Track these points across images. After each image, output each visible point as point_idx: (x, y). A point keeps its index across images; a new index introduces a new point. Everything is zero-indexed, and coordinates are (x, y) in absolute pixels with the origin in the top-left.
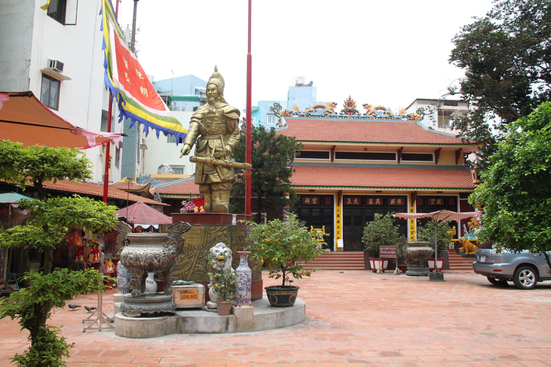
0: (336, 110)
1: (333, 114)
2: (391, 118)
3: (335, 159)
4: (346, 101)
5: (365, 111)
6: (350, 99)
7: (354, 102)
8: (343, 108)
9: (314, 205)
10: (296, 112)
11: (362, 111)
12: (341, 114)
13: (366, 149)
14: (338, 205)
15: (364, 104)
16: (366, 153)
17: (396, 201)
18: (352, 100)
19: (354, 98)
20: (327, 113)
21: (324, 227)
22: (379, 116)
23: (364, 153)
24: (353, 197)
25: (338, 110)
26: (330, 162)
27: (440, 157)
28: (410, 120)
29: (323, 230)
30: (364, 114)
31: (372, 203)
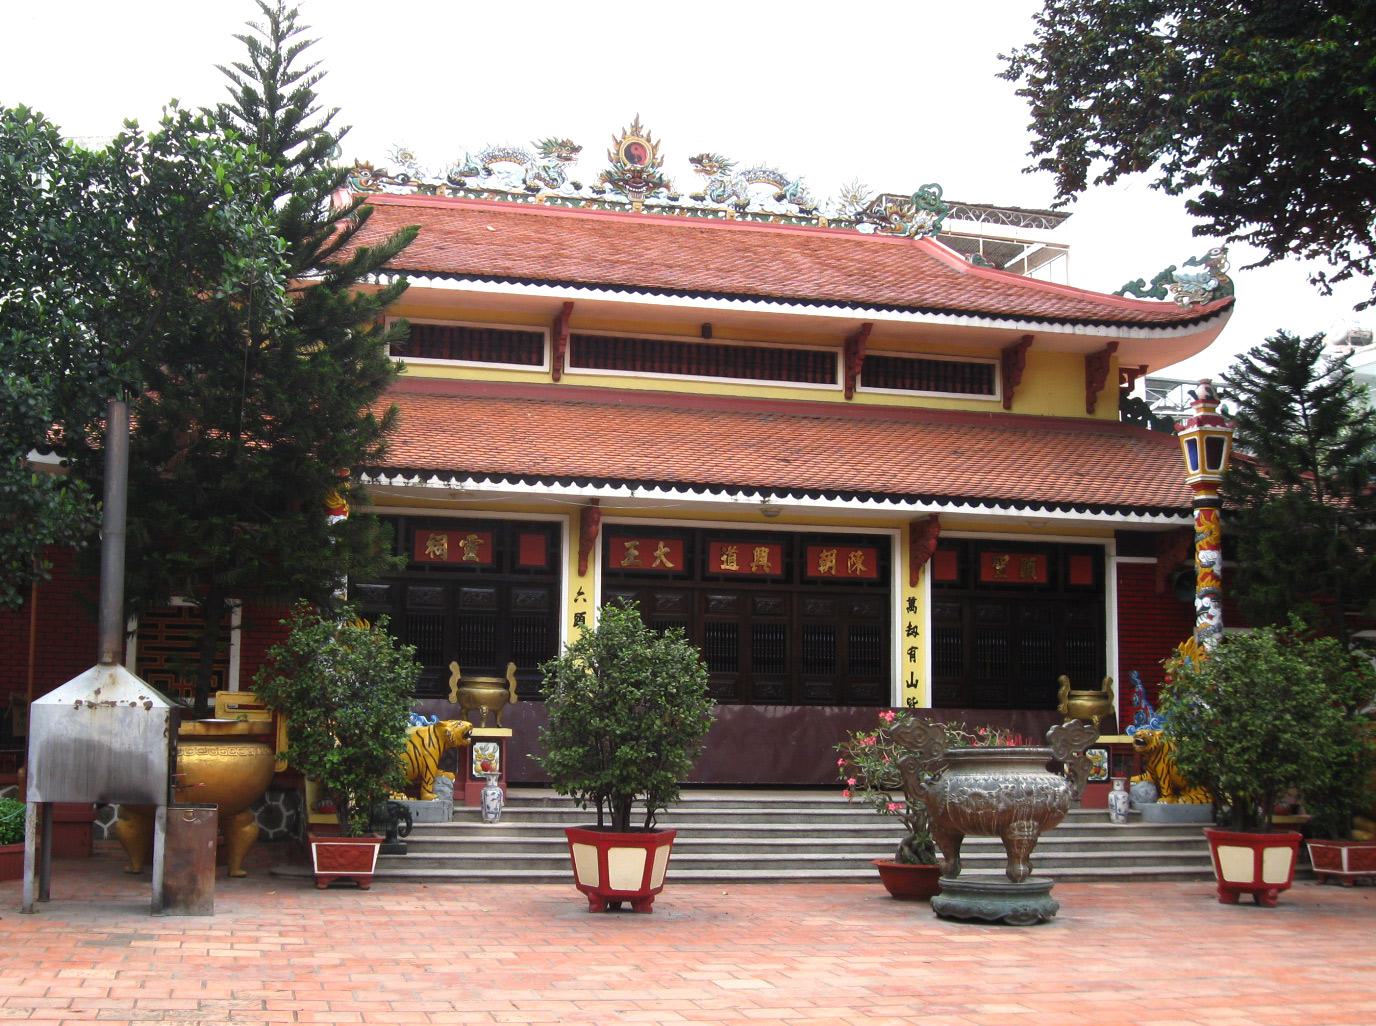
0: (572, 171)
2: (809, 220)
3: (568, 369)
6: (636, 128)
9: (468, 568)
11: (686, 183)
13: (706, 330)
14: (582, 572)
16: (708, 347)
17: (842, 561)
18: (644, 132)
19: (655, 127)
21: (512, 667)
22: (757, 209)
25: (589, 170)
27: (1027, 374)
29: (506, 686)
30: (696, 198)
31: (734, 567)
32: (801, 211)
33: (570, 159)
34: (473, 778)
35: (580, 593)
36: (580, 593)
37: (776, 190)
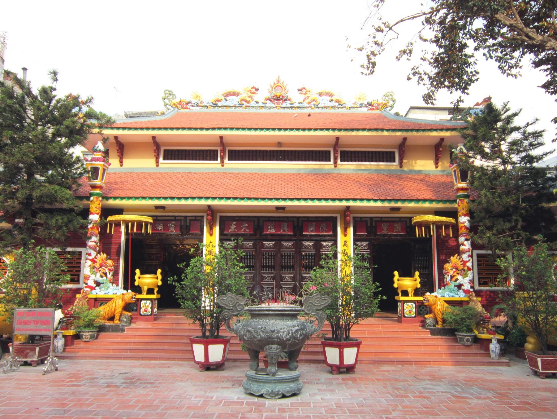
0: (257, 97)
1: (253, 104)
4: (272, 85)
5: (301, 98)
7: (285, 85)
8: (268, 95)
10: (196, 101)
11: (296, 98)
12: (264, 103)
13: (280, 144)
14: (211, 235)
15: (300, 88)
16: (281, 151)
20: (244, 102)
22: (323, 105)
23: (277, 151)
24: (240, 220)
26: (220, 166)
28: (372, 109)
29: (157, 278)
32: (340, 105)
33: (255, 93)
34: (141, 315)
35: (211, 242)
36: (211, 242)
37: (330, 98)
